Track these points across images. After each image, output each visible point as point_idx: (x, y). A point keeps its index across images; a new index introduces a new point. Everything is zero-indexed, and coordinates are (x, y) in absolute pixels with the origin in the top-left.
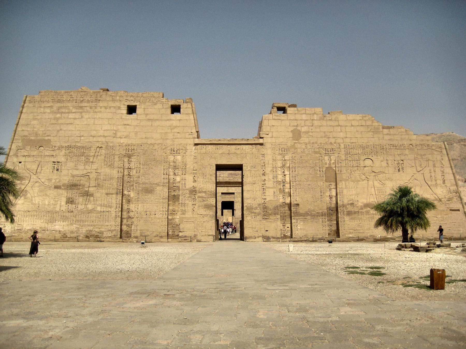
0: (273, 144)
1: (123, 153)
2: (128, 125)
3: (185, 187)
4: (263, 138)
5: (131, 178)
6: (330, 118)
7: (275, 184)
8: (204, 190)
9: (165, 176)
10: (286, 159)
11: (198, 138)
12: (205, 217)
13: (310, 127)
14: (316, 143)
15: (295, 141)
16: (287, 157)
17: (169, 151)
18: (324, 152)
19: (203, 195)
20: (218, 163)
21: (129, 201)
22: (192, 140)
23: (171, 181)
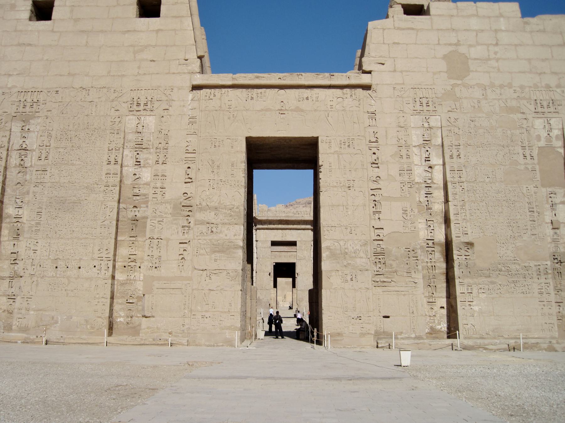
0: (398, 87)
1: (12, 110)
2: (30, 45)
4: (370, 72)
5: (25, 173)
8: (212, 204)
9: (112, 167)
10: (432, 124)
11: (202, 71)
12: (213, 277)
13: (491, 48)
14: (510, 86)
15: (453, 82)
16: (435, 121)
17: (124, 105)
18: (532, 107)
19: (210, 216)
21: (17, 235)
22: (187, 77)
23: (128, 181)
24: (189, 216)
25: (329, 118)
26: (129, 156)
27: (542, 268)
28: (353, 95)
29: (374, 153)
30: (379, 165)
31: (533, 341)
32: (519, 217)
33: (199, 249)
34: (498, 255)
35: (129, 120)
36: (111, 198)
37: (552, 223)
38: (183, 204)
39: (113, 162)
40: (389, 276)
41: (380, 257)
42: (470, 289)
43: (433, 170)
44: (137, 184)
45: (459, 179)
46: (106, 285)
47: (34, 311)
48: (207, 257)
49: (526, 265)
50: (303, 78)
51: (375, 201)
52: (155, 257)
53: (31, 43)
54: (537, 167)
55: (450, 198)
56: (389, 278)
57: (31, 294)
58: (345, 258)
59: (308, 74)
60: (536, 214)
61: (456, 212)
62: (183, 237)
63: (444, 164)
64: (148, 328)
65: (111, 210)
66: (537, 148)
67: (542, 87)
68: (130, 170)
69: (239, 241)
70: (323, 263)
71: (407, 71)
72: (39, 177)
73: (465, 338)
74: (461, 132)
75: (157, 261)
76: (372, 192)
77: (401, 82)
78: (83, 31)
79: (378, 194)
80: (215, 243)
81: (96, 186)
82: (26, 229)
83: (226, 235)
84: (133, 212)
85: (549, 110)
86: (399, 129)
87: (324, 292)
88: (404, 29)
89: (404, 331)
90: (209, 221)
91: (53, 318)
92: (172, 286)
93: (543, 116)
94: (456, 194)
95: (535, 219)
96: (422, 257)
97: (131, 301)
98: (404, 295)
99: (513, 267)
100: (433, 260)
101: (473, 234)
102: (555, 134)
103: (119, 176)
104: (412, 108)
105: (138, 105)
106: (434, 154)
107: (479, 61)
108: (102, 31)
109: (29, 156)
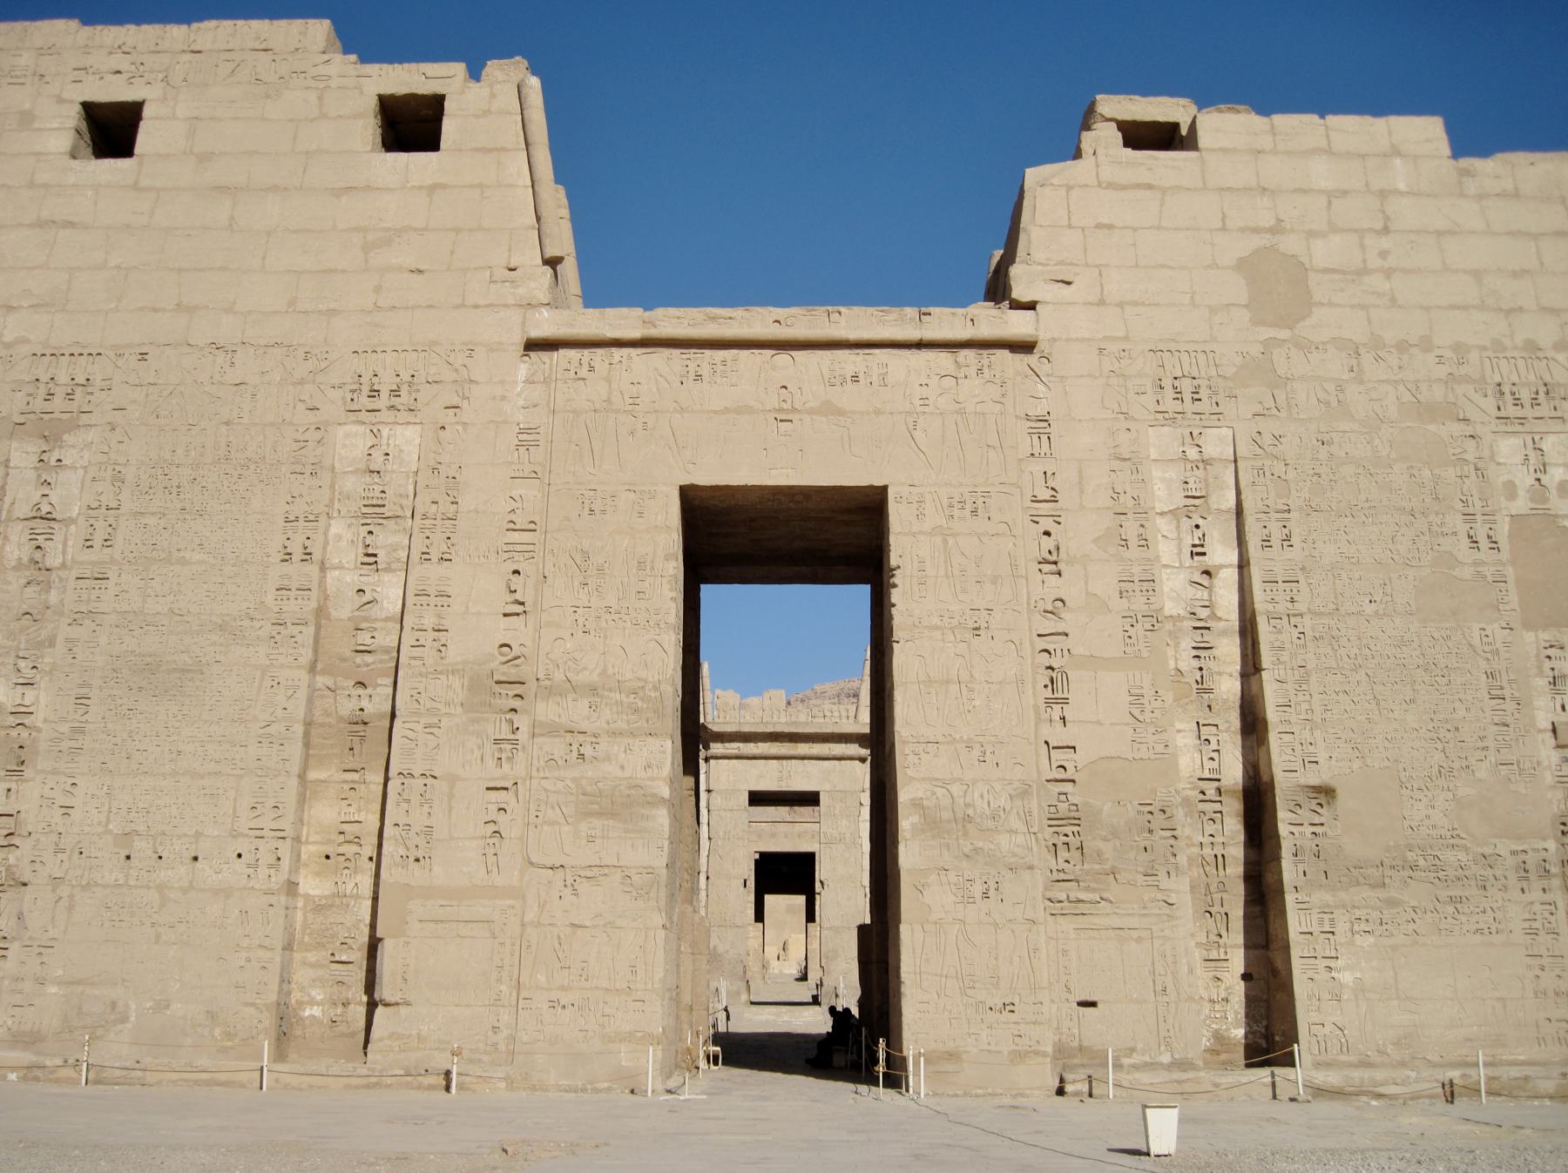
0: (1113, 348)
2: (70, 224)
4: (1031, 306)
6: (1508, 185)
7: (1137, 632)
9: (294, 568)
10: (1210, 450)
12: (583, 887)
13: (1369, 240)
17: (336, 394)
18: (1489, 404)
19: (576, 711)
20: (706, 477)
23: (343, 610)
24: (514, 710)
25: (917, 434)
26: (342, 540)
27: (1532, 860)
28: (986, 370)
29: (1047, 533)
30: (1061, 566)
31: (1514, 1072)
32: (1461, 713)
33: (543, 807)
34: (1406, 824)
35: (347, 436)
36: (291, 659)
37: (1554, 731)
38: (496, 678)
41: (1068, 830)
42: (1327, 922)
43: (1215, 581)
44: (366, 619)
45: (1290, 605)
46: (272, 911)
47: (59, 984)
48: (566, 828)
49: (1487, 850)
50: (843, 320)
51: (1050, 668)
52: (416, 828)
53: (75, 220)
54: (1510, 572)
55: (1266, 661)
56: (1094, 890)
57: (51, 934)
58: (966, 834)
59: (857, 310)
60: (1509, 706)
61: (1282, 701)
62: (498, 773)
63: (1243, 565)
64: (391, 1036)
65: (290, 692)
66: (1507, 519)
67: (1515, 348)
68: (348, 579)
69: (661, 783)
70: (901, 848)
71: (1136, 304)
72: (84, 597)
73: (1318, 1065)
74: (1291, 475)
75: (421, 841)
77: (1121, 334)
78: (220, 189)
80: (589, 789)
81: (247, 623)
82: (43, 746)
83: (622, 767)
84: (354, 700)
85: (1538, 412)
86: (1116, 464)
87: (905, 930)
88: (1124, 188)
89: (1140, 1046)
91: (114, 1005)
93: (1520, 428)
94: (1281, 648)
95: (1509, 720)
96: (1187, 831)
97: (344, 958)
98: (1139, 940)
99: (1449, 856)
100: (1219, 839)
101: (1333, 762)
102: (1557, 478)
103: (314, 594)
104: (1153, 406)
105: (374, 393)
106: (1216, 534)
107: (1337, 277)
108: (274, 189)
109: (59, 537)
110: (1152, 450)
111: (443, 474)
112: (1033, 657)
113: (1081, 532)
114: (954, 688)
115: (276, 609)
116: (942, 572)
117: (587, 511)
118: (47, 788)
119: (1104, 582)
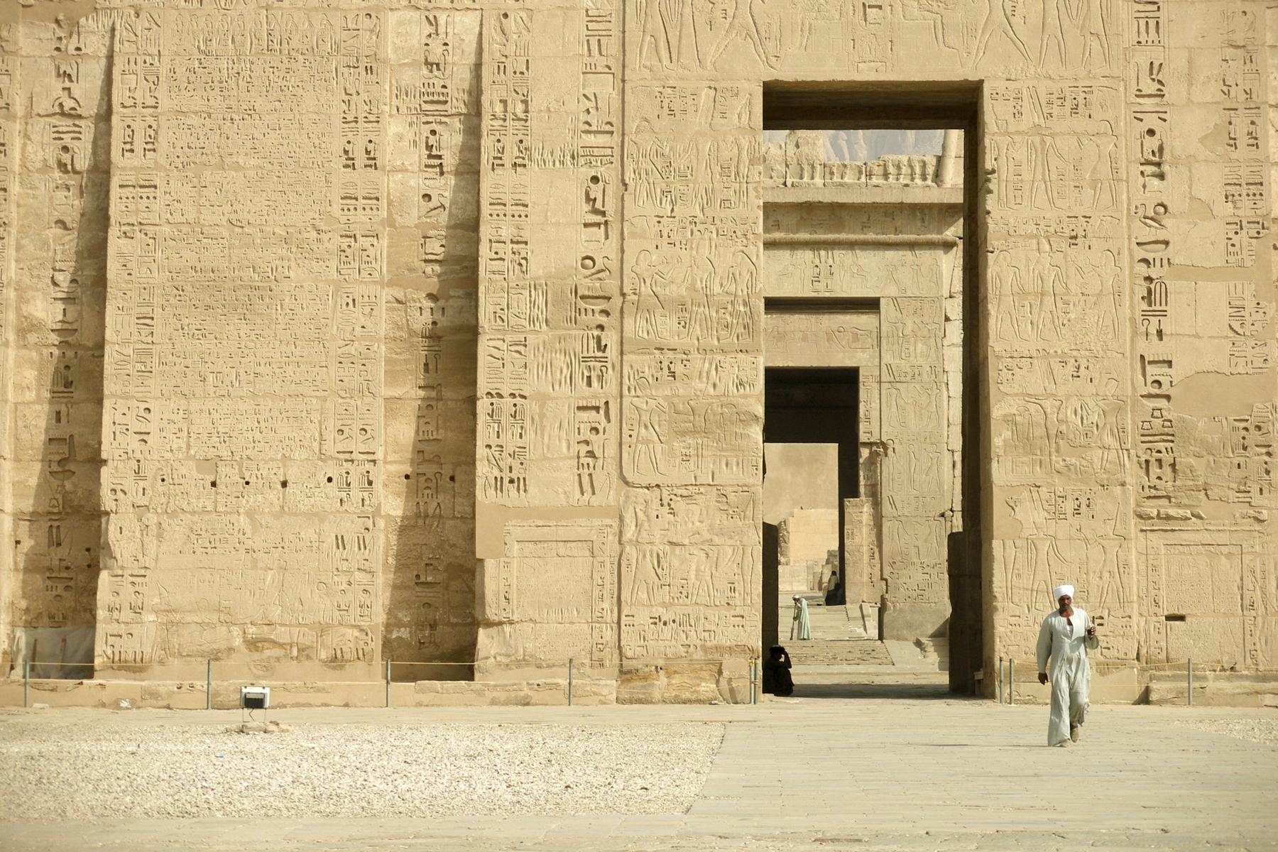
3: (522, 263)
9: (360, 179)
12: (680, 505)
19: (667, 327)
29: (1151, 132)
30: (1166, 168)
33: (636, 427)
39: (361, 159)
40: (1185, 501)
41: (1161, 446)
48: (659, 447)
56: (1186, 506)
68: (412, 183)
69: (752, 401)
70: (994, 464)
72: (132, 207)
76: (1140, 253)
79: (1158, 256)
86: (1230, 52)
90: (660, 342)
92: (563, 533)
110: (1269, 34)
111: (510, 70)
112: (1132, 268)
113: (1187, 130)
114: (1049, 300)
115: (343, 220)
116: (1039, 176)
117: (666, 111)
118: (119, 413)
119: (1209, 182)
